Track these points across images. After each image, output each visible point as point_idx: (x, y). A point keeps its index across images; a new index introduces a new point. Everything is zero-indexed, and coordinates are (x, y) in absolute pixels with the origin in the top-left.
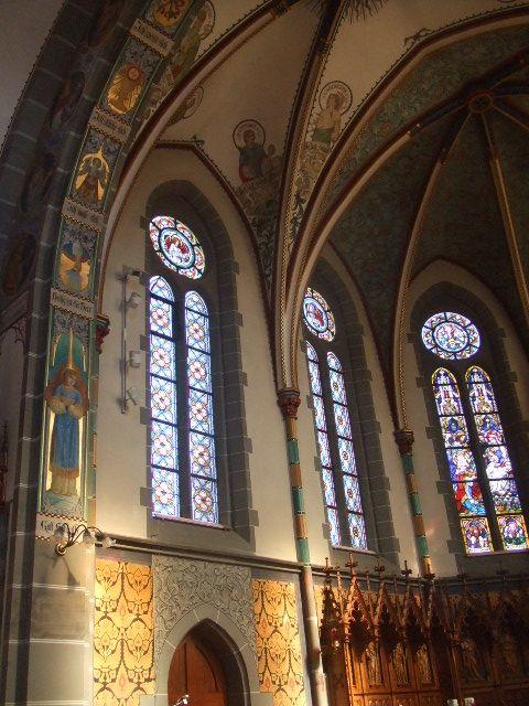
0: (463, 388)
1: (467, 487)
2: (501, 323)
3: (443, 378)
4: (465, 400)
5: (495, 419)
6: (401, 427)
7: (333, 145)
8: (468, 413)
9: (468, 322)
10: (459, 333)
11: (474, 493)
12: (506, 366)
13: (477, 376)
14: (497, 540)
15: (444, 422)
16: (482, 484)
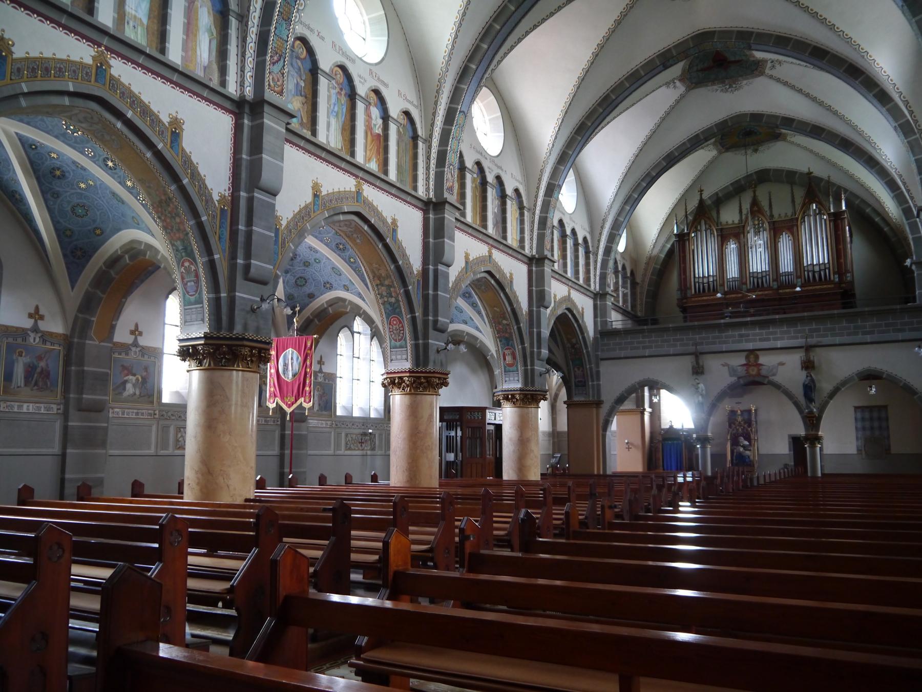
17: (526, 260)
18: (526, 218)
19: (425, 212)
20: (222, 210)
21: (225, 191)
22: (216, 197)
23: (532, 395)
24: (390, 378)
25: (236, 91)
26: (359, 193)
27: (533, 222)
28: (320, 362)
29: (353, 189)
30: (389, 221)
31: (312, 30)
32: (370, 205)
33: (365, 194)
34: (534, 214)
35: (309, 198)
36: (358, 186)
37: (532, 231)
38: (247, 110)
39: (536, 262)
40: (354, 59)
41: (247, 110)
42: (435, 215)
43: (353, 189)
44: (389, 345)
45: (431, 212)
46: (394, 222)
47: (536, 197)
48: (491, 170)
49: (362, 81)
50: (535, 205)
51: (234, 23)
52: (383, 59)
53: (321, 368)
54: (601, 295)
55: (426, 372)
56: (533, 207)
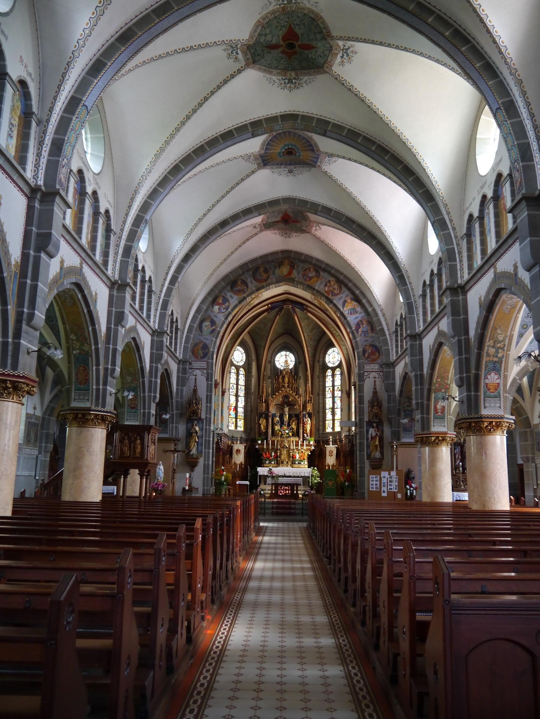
0: (238, 374)
1: (232, 408)
2: (254, 357)
3: (233, 370)
4: (238, 380)
5: (243, 388)
6: (224, 387)
7: (250, 308)
8: (237, 384)
9: (243, 351)
10: (241, 355)
11: (234, 410)
12: (251, 372)
13: (242, 372)
14: (236, 426)
15: (231, 385)
16: (236, 409)
17: (151, 332)
20: (15, 272)
24: (73, 414)
26: (81, 268)
27: (157, 304)
29: (79, 266)
30: (94, 294)
32: (84, 279)
33: (84, 270)
34: (159, 298)
36: (81, 264)
37: (156, 310)
38: (39, 196)
39: (156, 334)
40: (88, 168)
41: (39, 196)
42: (117, 293)
43: (79, 266)
44: (73, 388)
45: (115, 290)
46: (96, 294)
47: (163, 286)
50: (161, 291)
52: (101, 171)
54: (183, 362)
55: (104, 412)
56: (158, 292)
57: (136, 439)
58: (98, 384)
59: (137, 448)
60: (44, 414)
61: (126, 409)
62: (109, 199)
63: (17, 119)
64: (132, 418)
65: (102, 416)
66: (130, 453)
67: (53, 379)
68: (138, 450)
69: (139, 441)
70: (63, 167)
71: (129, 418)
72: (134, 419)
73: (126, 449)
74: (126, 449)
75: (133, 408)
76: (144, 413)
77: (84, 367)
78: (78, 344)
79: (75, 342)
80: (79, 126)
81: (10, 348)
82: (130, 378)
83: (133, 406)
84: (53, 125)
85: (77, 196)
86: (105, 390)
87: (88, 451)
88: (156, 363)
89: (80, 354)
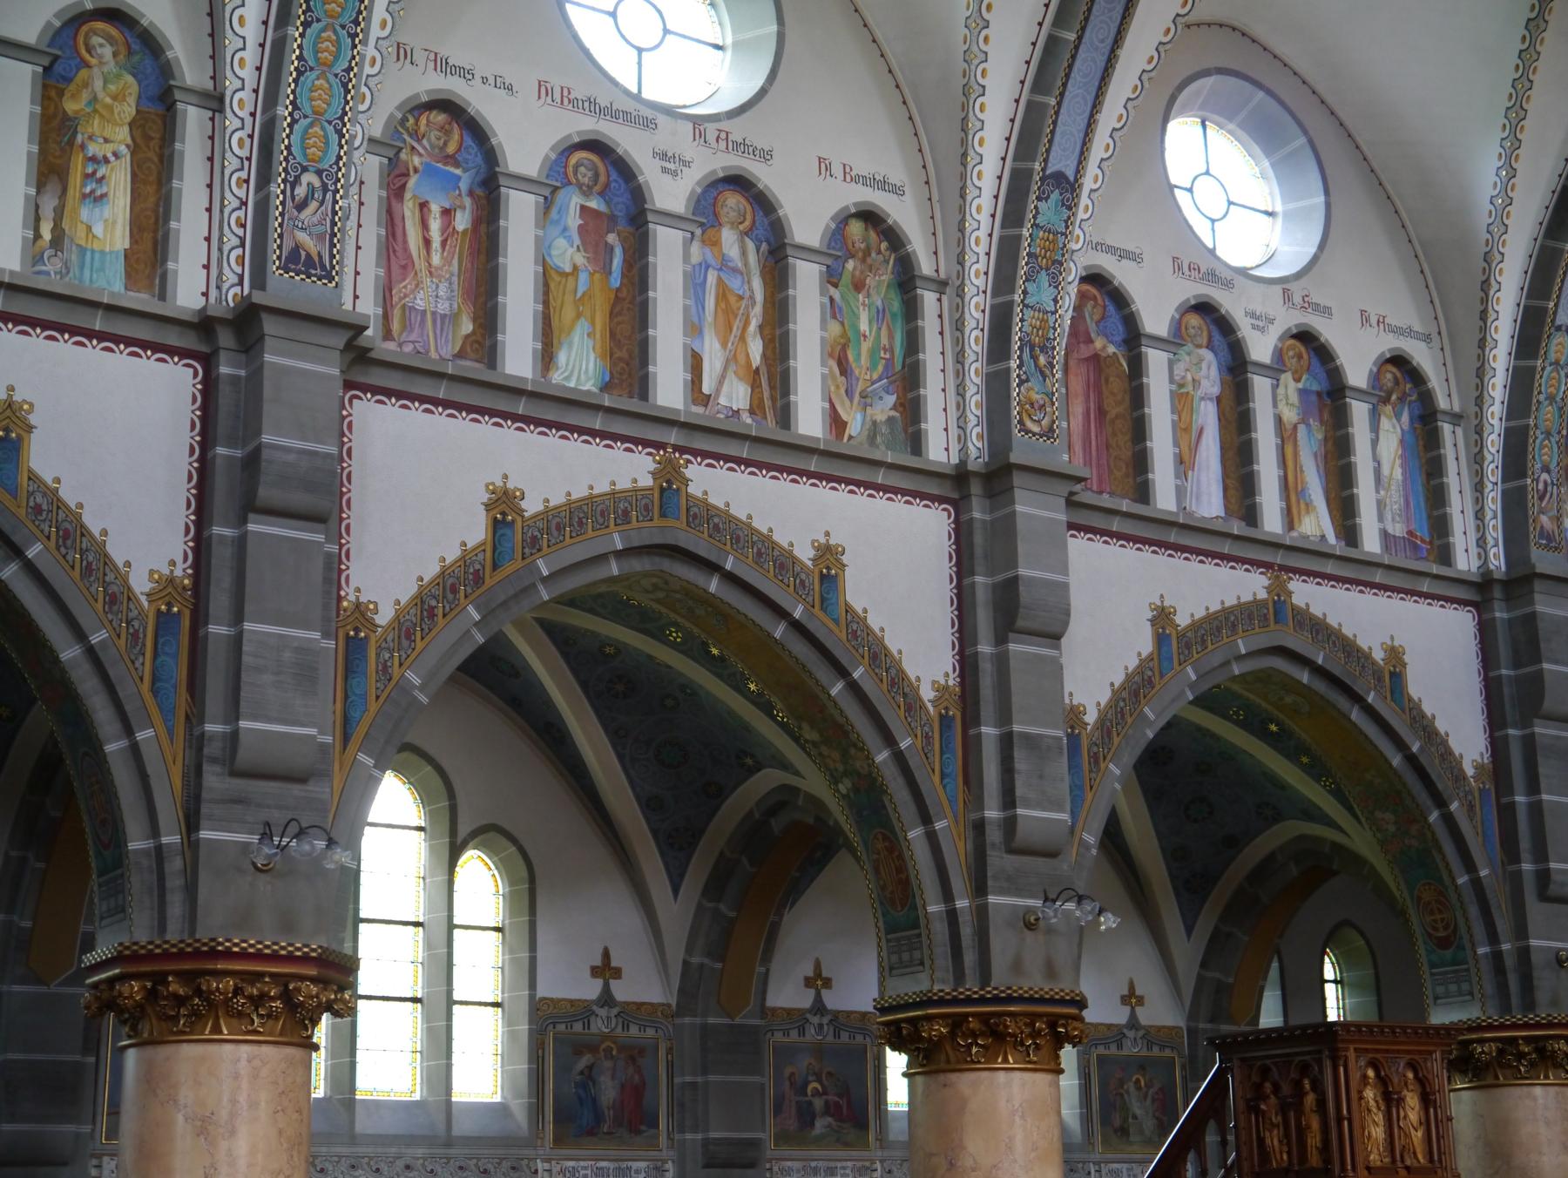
18: (1448, 452)
19: (958, 505)
21: (173, 563)
22: (140, 584)
23: (1539, 1045)
25: (206, 294)
27: (1478, 459)
28: (818, 981)
30: (805, 554)
31: (465, 73)
34: (1479, 430)
35: (477, 531)
45: (975, 502)
48: (1262, 321)
49: (671, 166)
51: (193, 119)
53: (818, 998)
55: (982, 1001)
56: (1474, 409)
57: (1300, 1094)
58: (948, 896)
59: (1309, 1127)
60: (1192, 1016)
61: (1422, 951)
62: (862, 168)
63: (123, 134)
64: (1453, 988)
65: (984, 1018)
66: (1289, 1153)
67: (1173, 878)
68: (1314, 1140)
69: (1310, 1099)
70: (301, 206)
71: (1440, 990)
72: (1460, 994)
73: (1273, 1140)
74: (1273, 1140)
75: (1444, 943)
76: (1497, 956)
77: (885, 838)
78: (836, 755)
79: (824, 750)
80: (337, 44)
81: (175, 865)
82: (1389, 816)
83: (1442, 934)
84: (250, 84)
85: (612, 238)
86: (982, 912)
87: (951, 1165)
88: (1525, 723)
89: (856, 790)
